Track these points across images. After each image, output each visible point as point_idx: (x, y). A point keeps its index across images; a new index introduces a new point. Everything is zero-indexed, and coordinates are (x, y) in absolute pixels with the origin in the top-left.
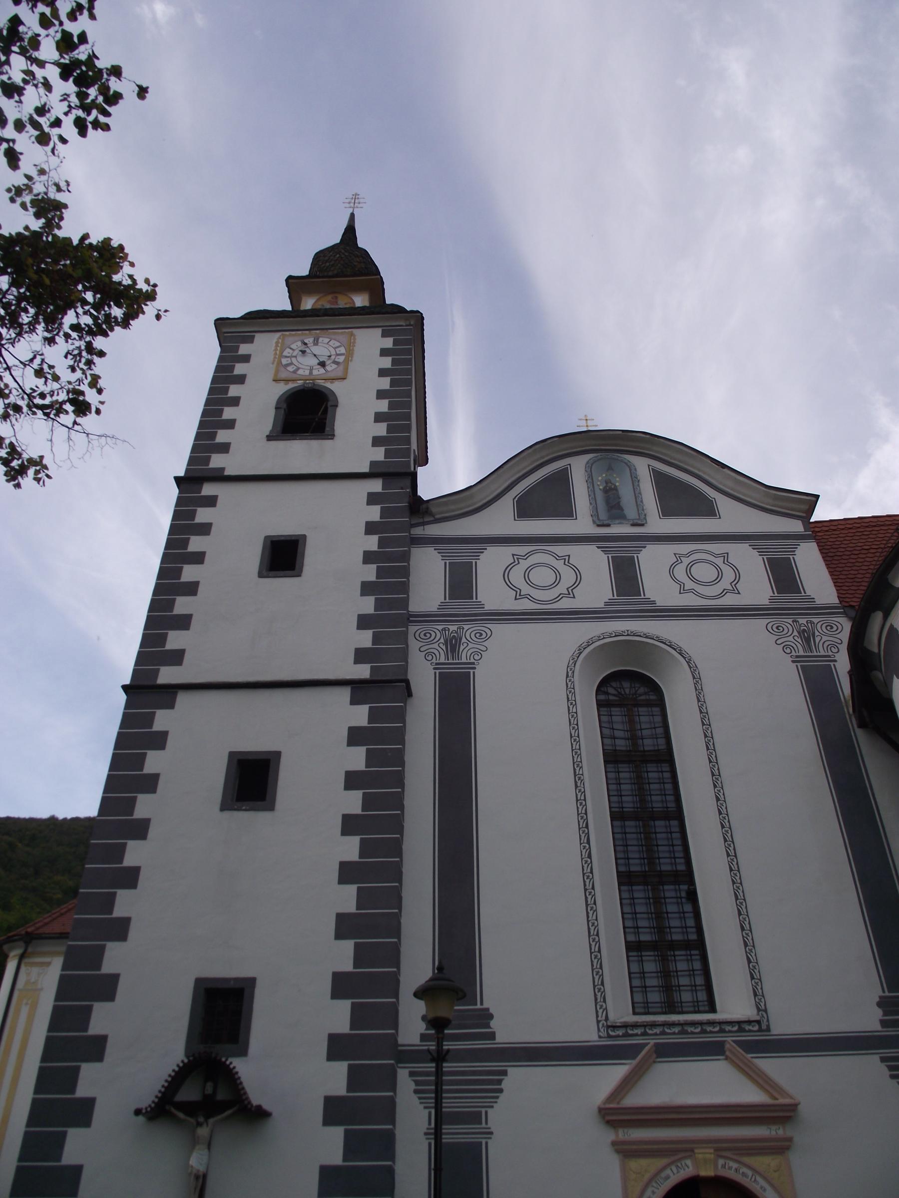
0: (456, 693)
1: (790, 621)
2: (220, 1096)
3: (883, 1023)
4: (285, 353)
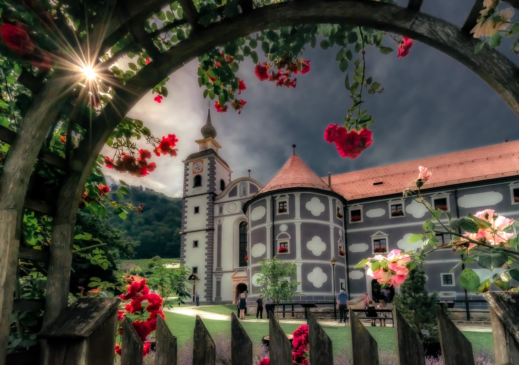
0: (220, 228)
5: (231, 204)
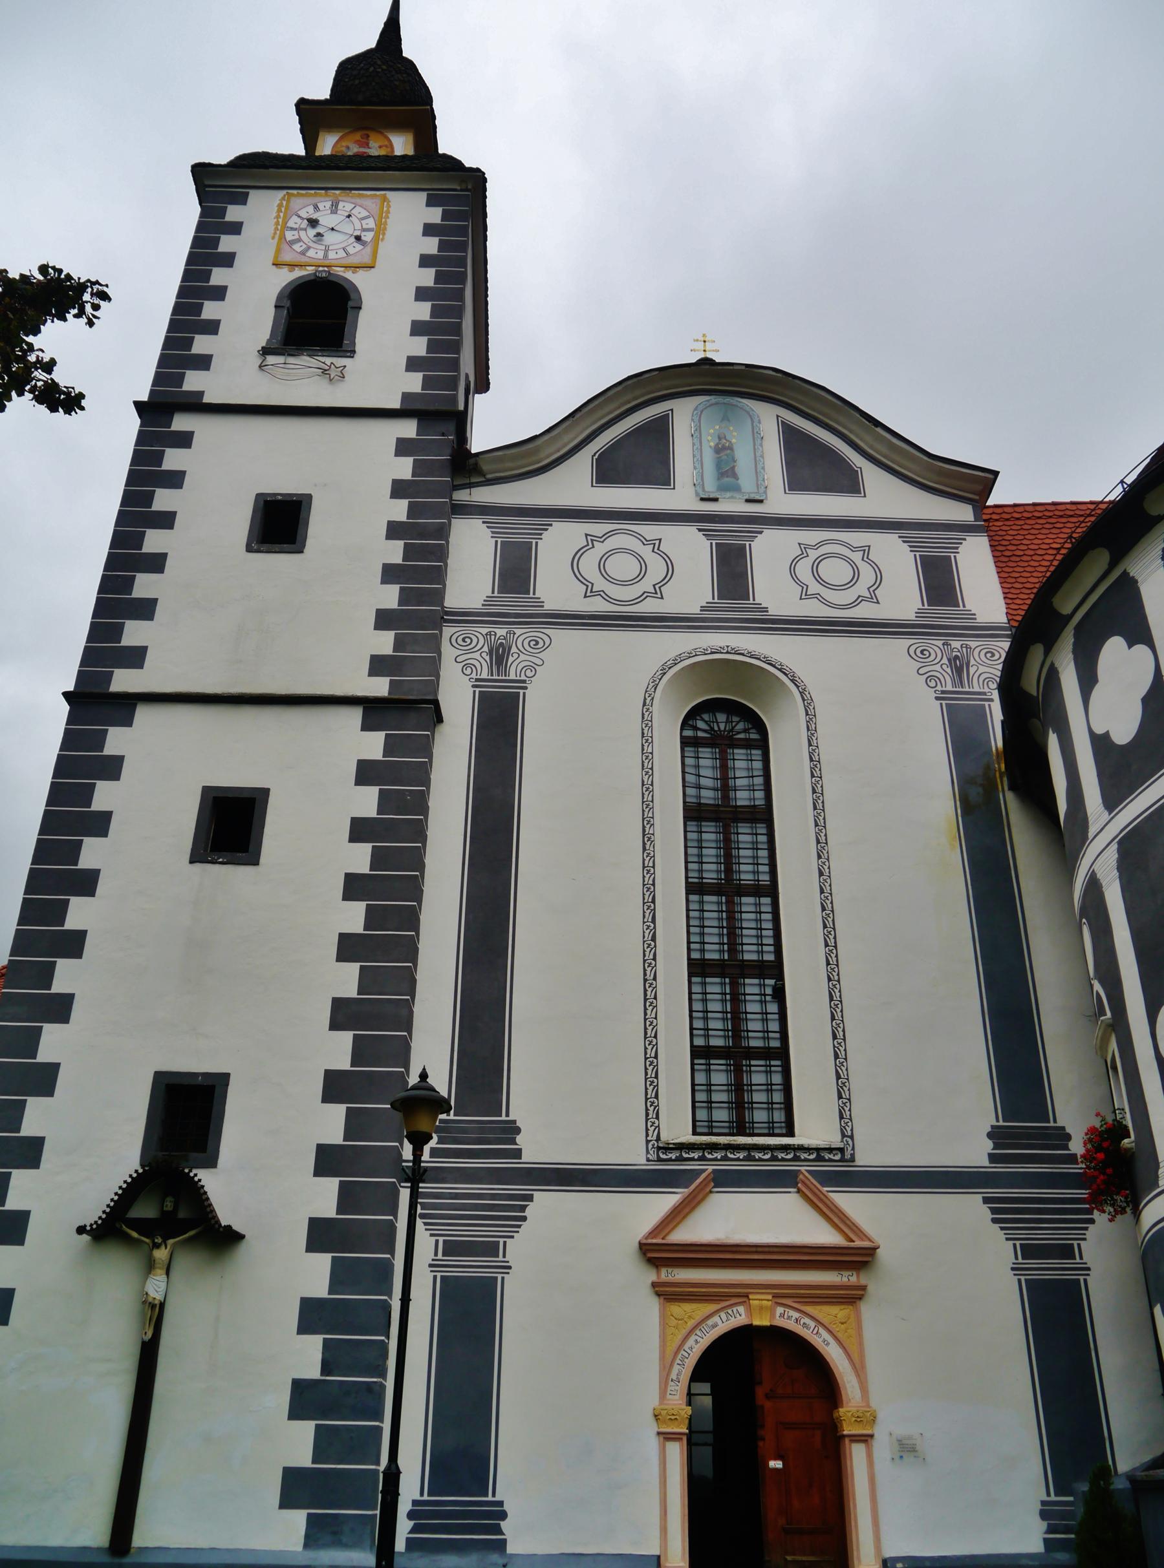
0: (499, 720)
1: (940, 643)
2: (182, 1214)
3: (993, 1158)
4: (291, 224)
5: (624, 538)
